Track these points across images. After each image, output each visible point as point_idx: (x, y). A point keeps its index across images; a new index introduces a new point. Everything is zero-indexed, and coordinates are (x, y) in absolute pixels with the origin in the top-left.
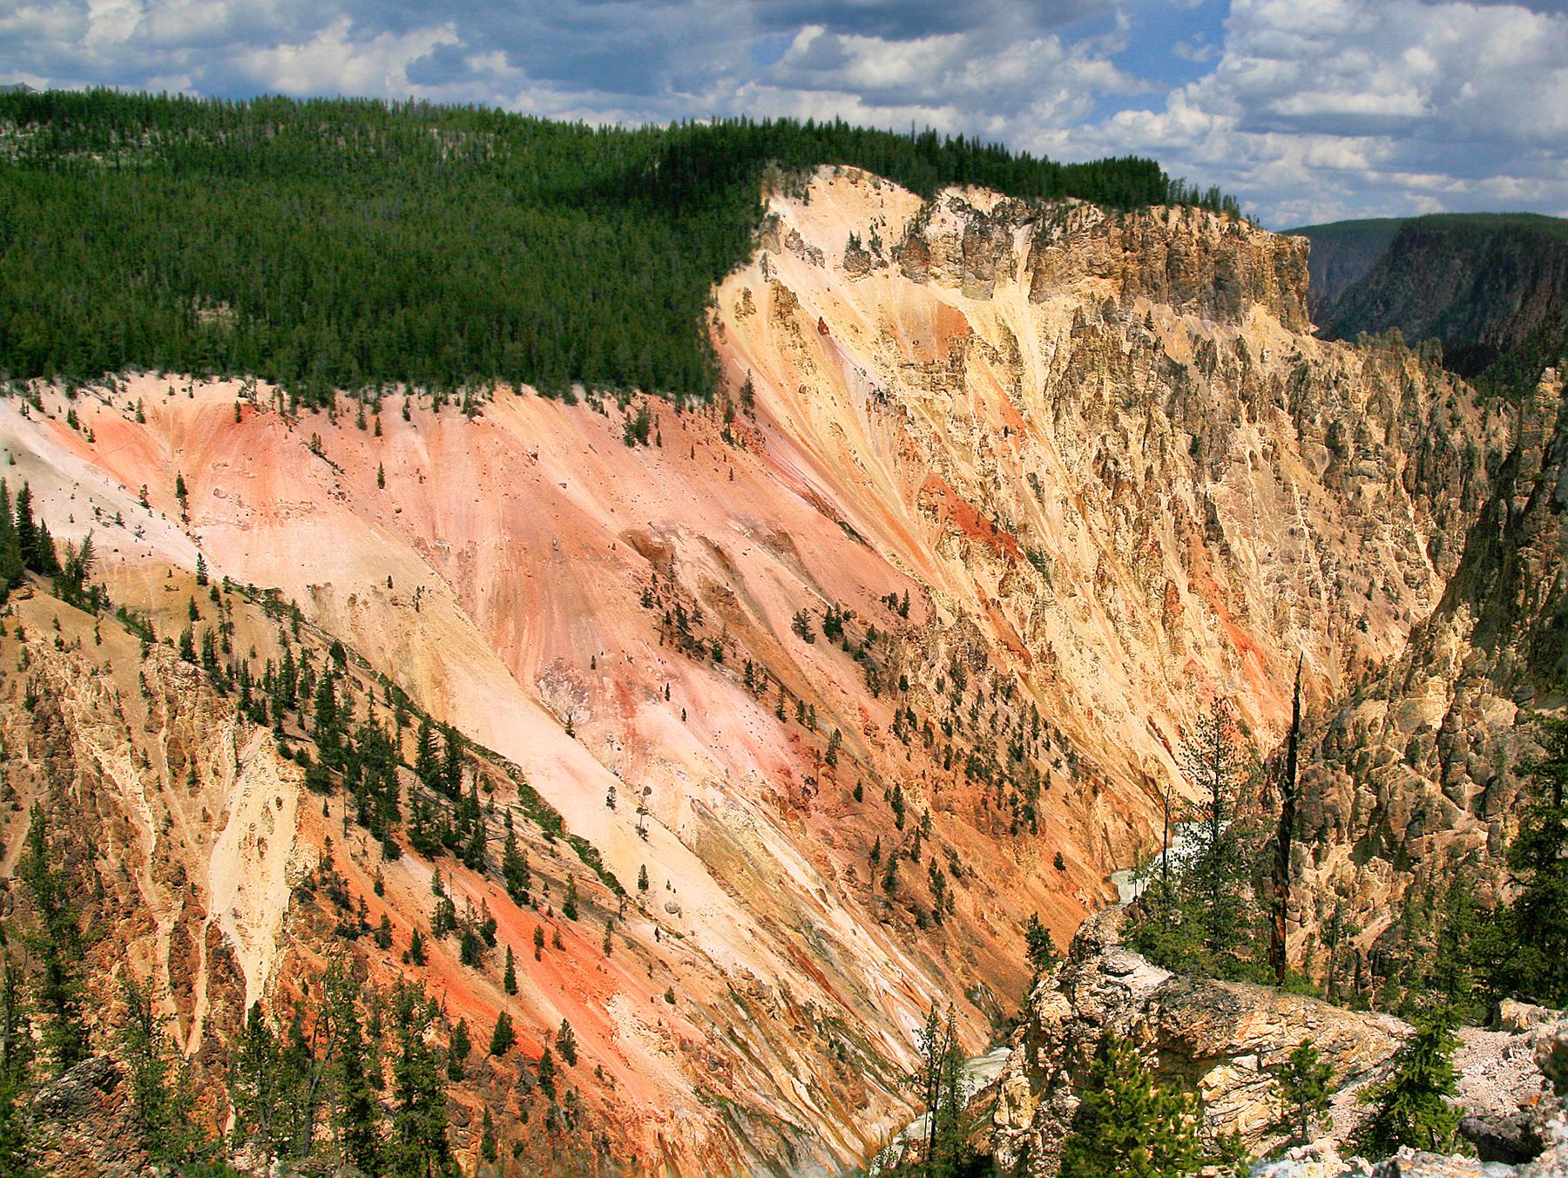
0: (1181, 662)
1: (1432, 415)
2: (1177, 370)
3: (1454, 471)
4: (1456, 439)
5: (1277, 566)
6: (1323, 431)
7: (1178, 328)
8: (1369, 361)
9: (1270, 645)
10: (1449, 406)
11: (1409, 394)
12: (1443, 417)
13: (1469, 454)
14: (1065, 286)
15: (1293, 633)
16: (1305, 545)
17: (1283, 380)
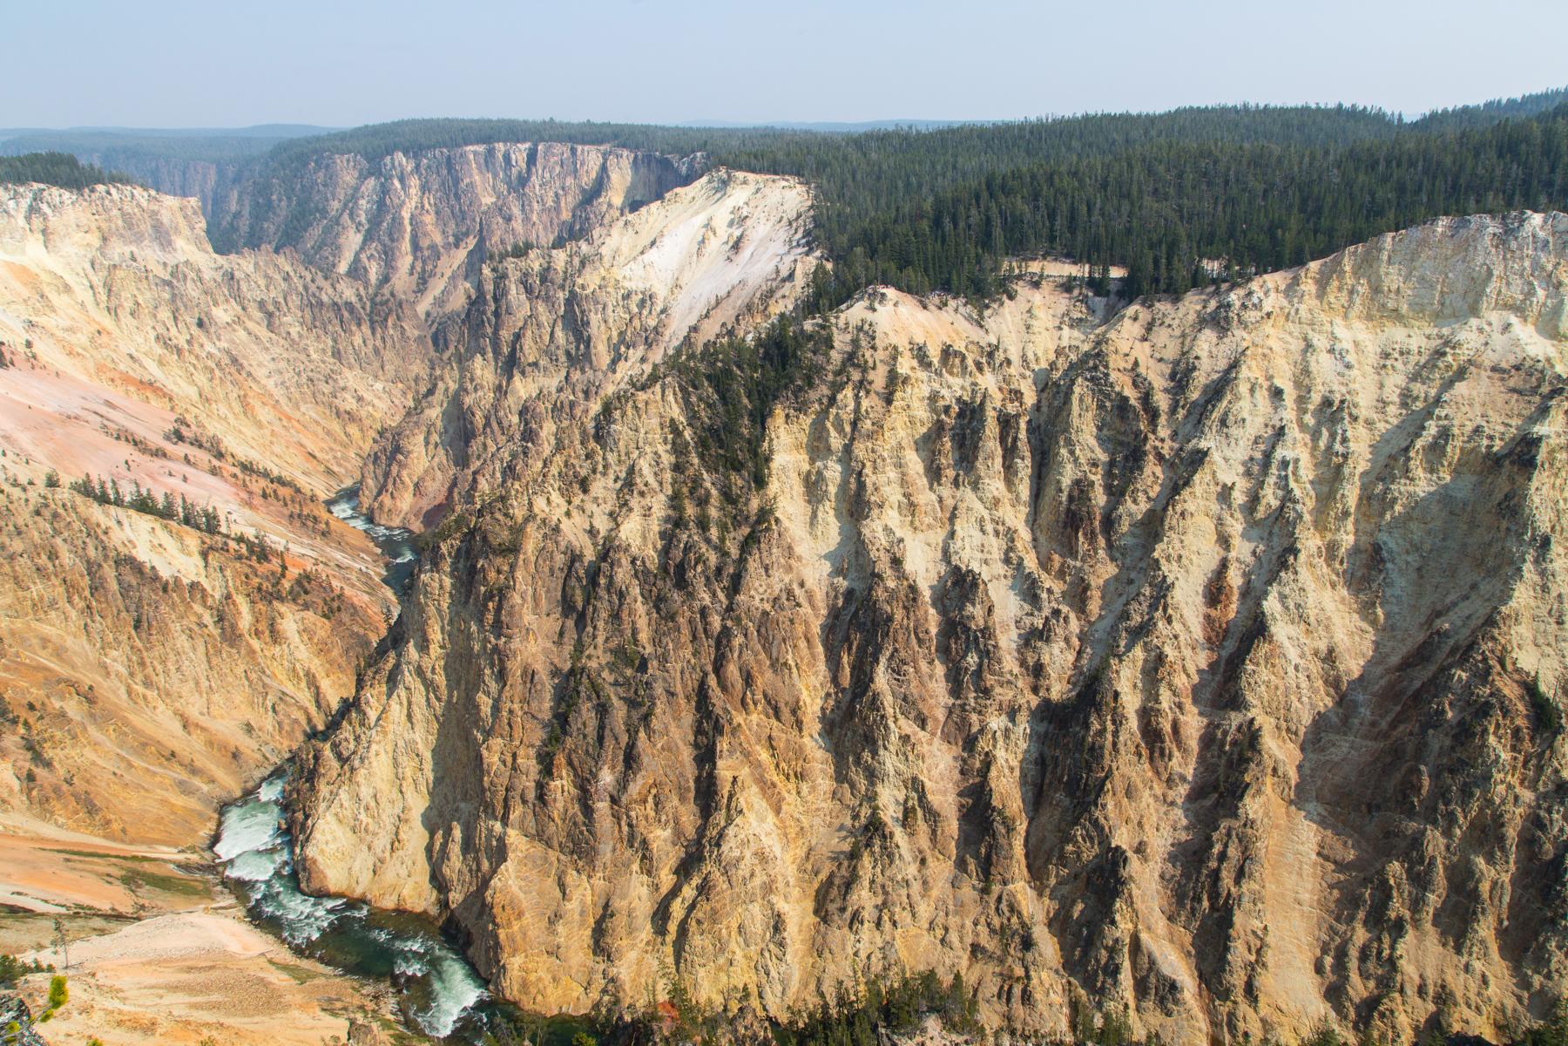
0: (267, 432)
1: (306, 288)
2: (169, 284)
3: (331, 315)
4: (325, 298)
5: (276, 377)
6: (255, 305)
7: (151, 255)
8: (256, 264)
9: (297, 415)
10: (313, 281)
11: (287, 278)
12: (313, 288)
13: (335, 304)
14: (67, 240)
15: (303, 409)
16: (283, 365)
17: (219, 279)
